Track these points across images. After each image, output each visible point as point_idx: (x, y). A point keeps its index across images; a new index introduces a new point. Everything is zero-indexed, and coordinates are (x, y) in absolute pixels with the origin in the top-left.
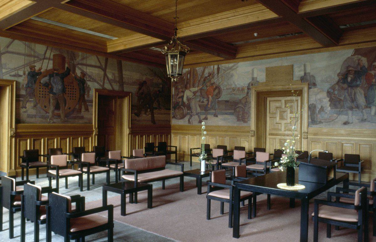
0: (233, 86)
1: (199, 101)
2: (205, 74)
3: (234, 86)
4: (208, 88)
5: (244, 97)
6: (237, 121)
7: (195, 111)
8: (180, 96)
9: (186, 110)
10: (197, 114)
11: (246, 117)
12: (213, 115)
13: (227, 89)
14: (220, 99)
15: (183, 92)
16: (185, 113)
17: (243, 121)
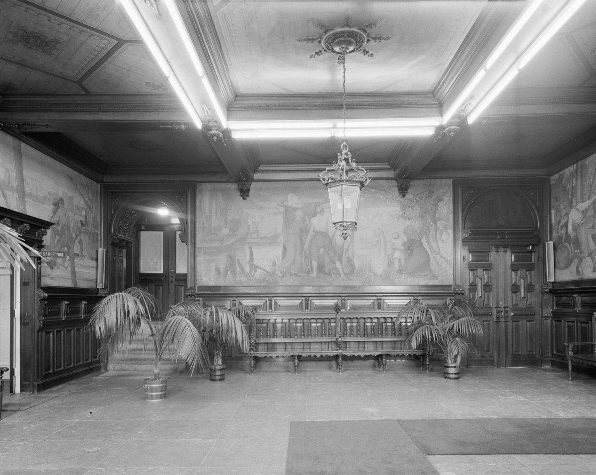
7: (586, 251)
8: (563, 224)
9: (573, 249)
10: (590, 255)
15: (567, 215)
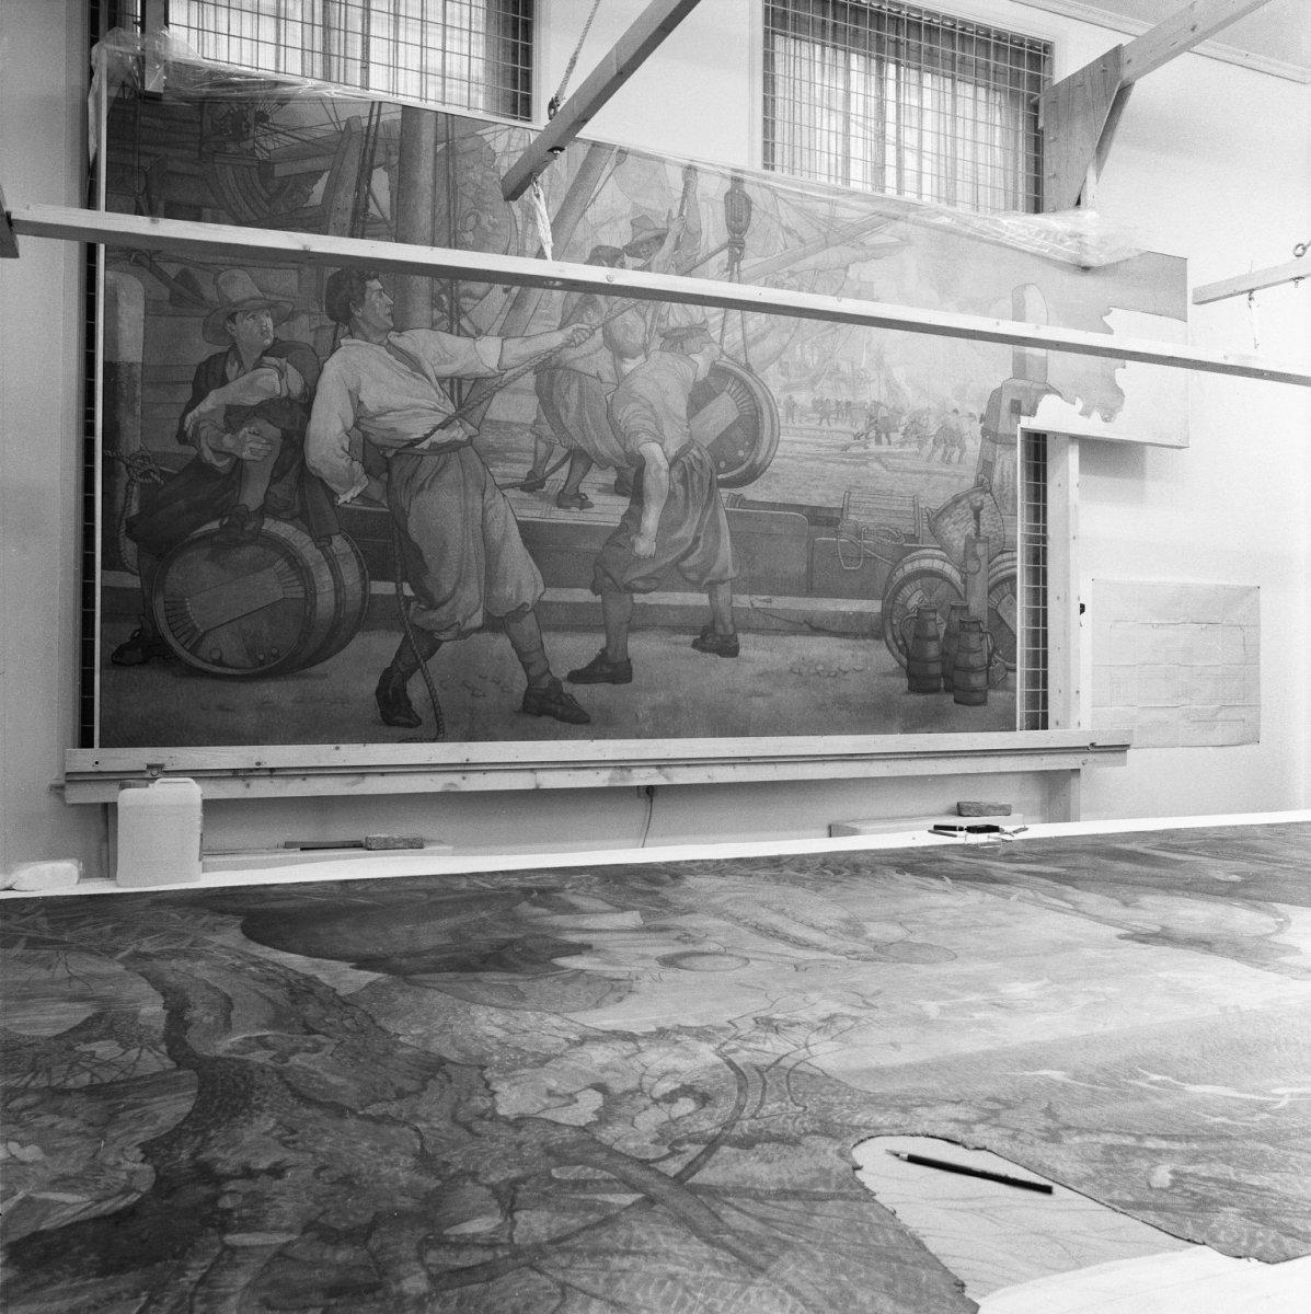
0: (872, 393)
1: (532, 484)
2: (593, 213)
3: (884, 391)
4: (629, 366)
5: (956, 501)
6: (912, 689)
7: (471, 594)
8: (253, 400)
11: (975, 660)
12: (689, 638)
13: (821, 407)
14: (751, 492)
16: (325, 601)
17: (948, 690)
